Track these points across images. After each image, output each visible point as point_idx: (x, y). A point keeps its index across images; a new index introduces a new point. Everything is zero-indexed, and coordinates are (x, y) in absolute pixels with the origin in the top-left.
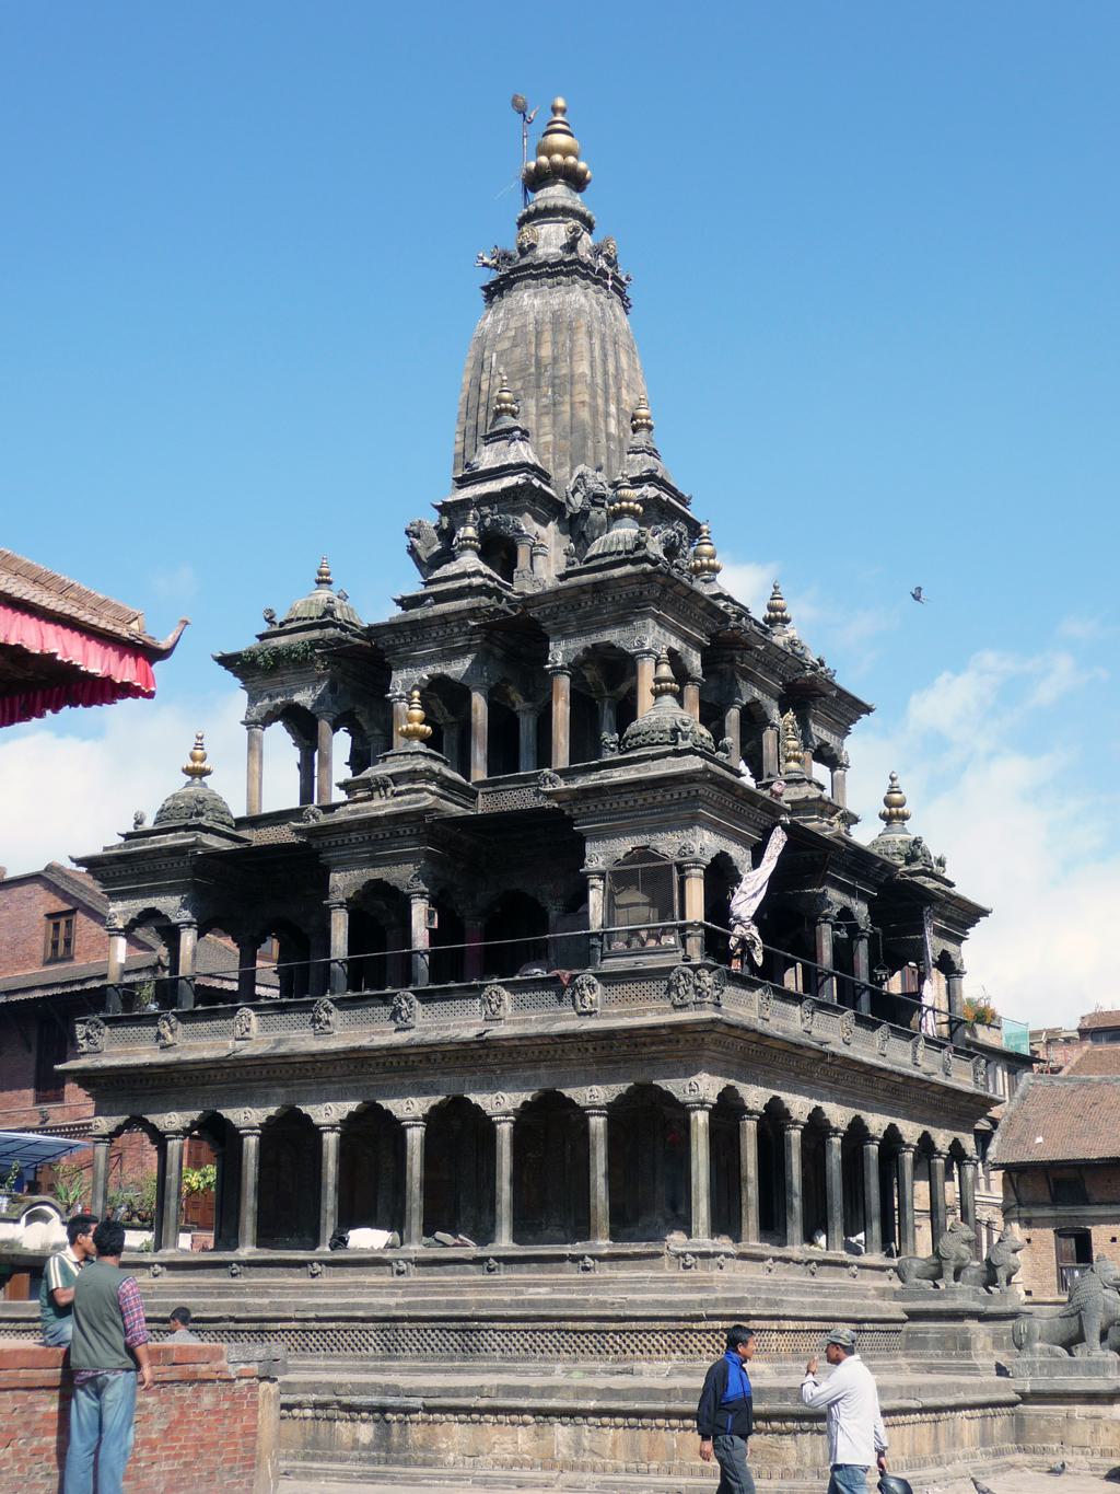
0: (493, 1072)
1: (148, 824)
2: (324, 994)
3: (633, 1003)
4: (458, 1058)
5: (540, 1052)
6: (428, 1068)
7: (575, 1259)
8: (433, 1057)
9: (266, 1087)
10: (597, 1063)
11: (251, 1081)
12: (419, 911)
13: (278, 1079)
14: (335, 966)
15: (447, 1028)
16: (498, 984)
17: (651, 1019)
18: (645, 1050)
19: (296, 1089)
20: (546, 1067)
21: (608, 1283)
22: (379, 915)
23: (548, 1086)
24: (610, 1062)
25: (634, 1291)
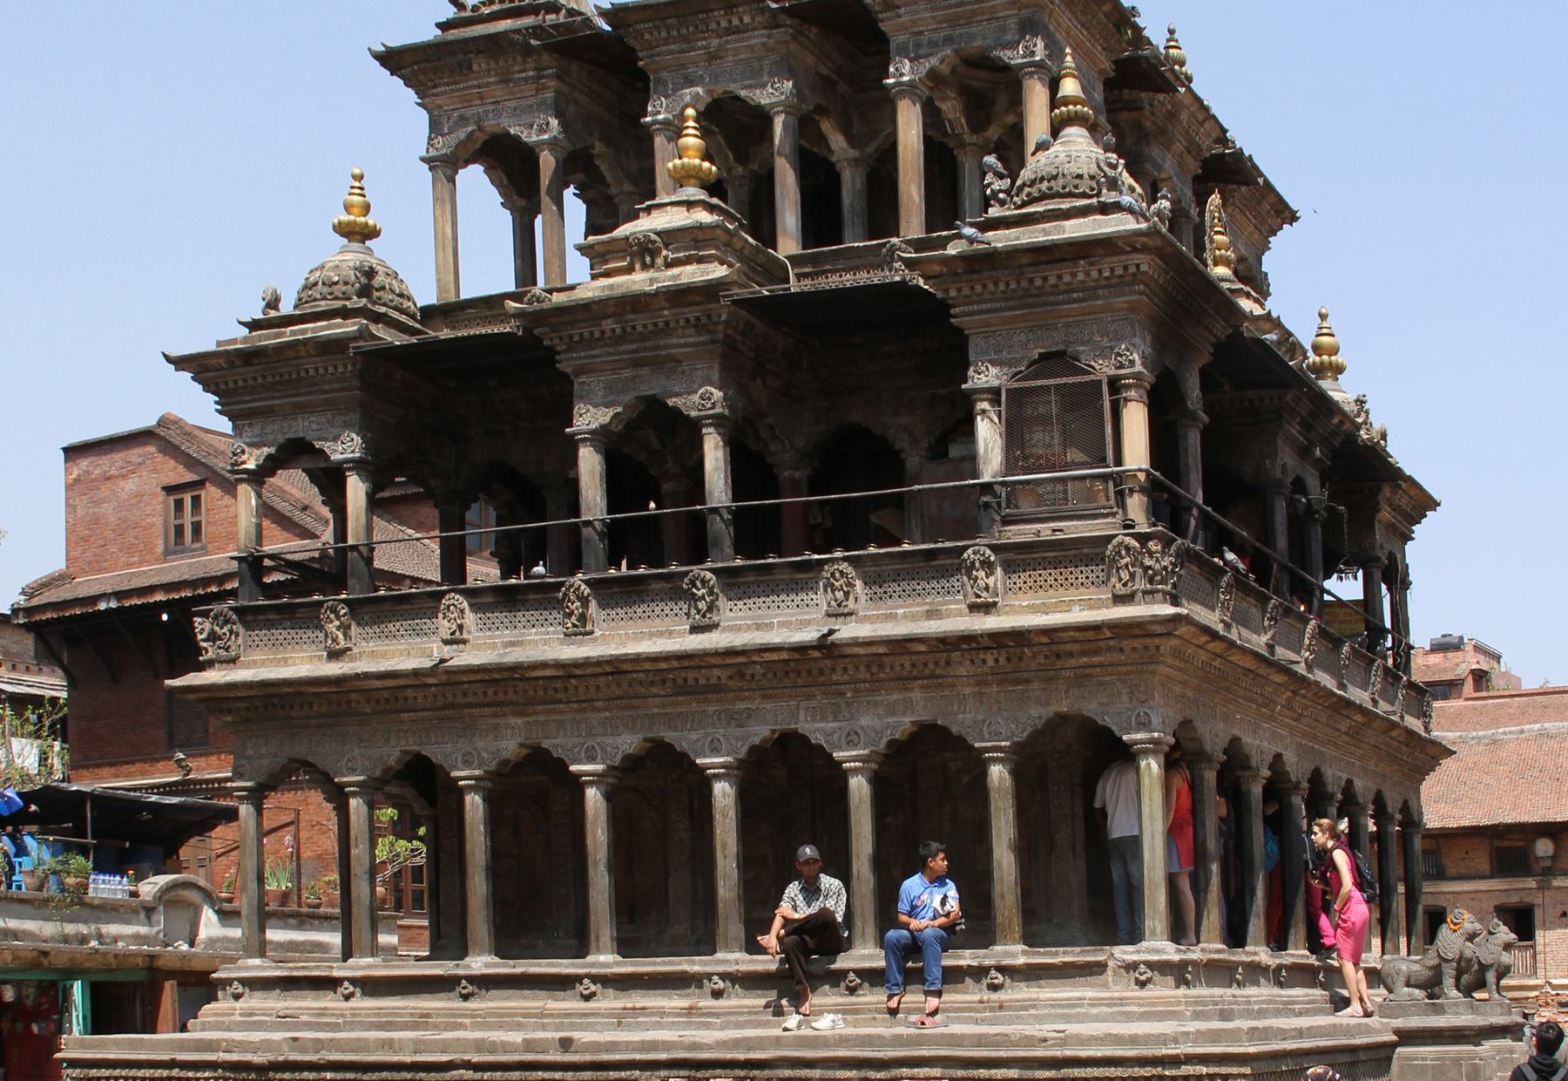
0: (842, 694)
1: (286, 308)
2: (573, 574)
3: (1051, 591)
4: (787, 673)
5: (914, 665)
6: (741, 689)
7: (979, 973)
8: (749, 672)
9: (495, 716)
10: (1000, 683)
11: (471, 706)
12: (714, 454)
13: (512, 703)
14: (586, 531)
15: (770, 626)
16: (845, 559)
17: (1079, 616)
18: (1072, 662)
19: (541, 718)
20: (922, 687)
21: (1025, 1008)
22: (651, 452)
23: (926, 717)
24: (1018, 682)
25: (1067, 1018)
